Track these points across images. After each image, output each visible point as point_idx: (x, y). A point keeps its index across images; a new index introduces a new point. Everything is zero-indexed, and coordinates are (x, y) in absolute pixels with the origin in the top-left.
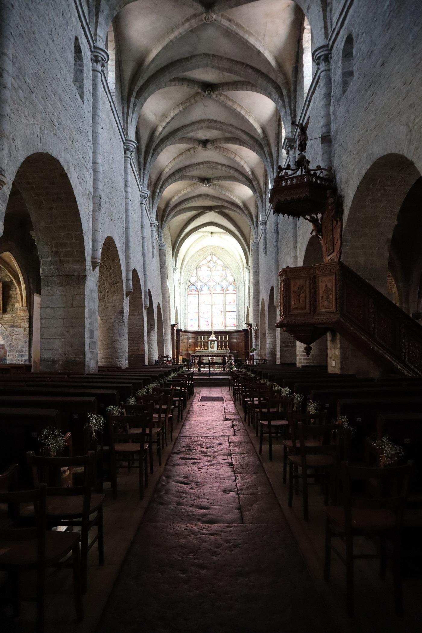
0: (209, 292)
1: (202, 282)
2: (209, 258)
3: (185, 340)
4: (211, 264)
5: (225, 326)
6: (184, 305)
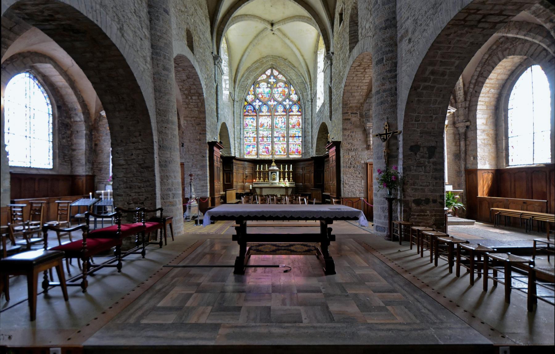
0: (269, 114)
1: (260, 101)
2: (269, 72)
3: (241, 171)
4: (272, 80)
6: (239, 128)
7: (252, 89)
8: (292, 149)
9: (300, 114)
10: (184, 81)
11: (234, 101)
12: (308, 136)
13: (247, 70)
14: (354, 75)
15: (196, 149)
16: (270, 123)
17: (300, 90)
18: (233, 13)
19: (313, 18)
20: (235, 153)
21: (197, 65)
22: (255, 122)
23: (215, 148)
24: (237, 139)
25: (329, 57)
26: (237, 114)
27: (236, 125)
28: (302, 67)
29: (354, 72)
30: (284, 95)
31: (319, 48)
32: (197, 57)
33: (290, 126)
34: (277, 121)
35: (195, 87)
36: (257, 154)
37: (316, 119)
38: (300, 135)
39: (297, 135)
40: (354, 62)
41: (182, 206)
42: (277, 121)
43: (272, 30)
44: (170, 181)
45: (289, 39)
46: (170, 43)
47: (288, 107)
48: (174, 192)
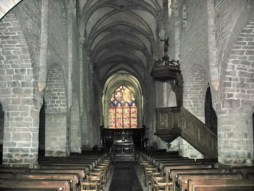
0: (121, 107)
1: (117, 101)
2: (121, 87)
5: (130, 126)
6: (107, 114)
9: (136, 107)
12: (140, 118)
16: (122, 111)
36: (116, 126)
38: (136, 117)
47: (130, 103)
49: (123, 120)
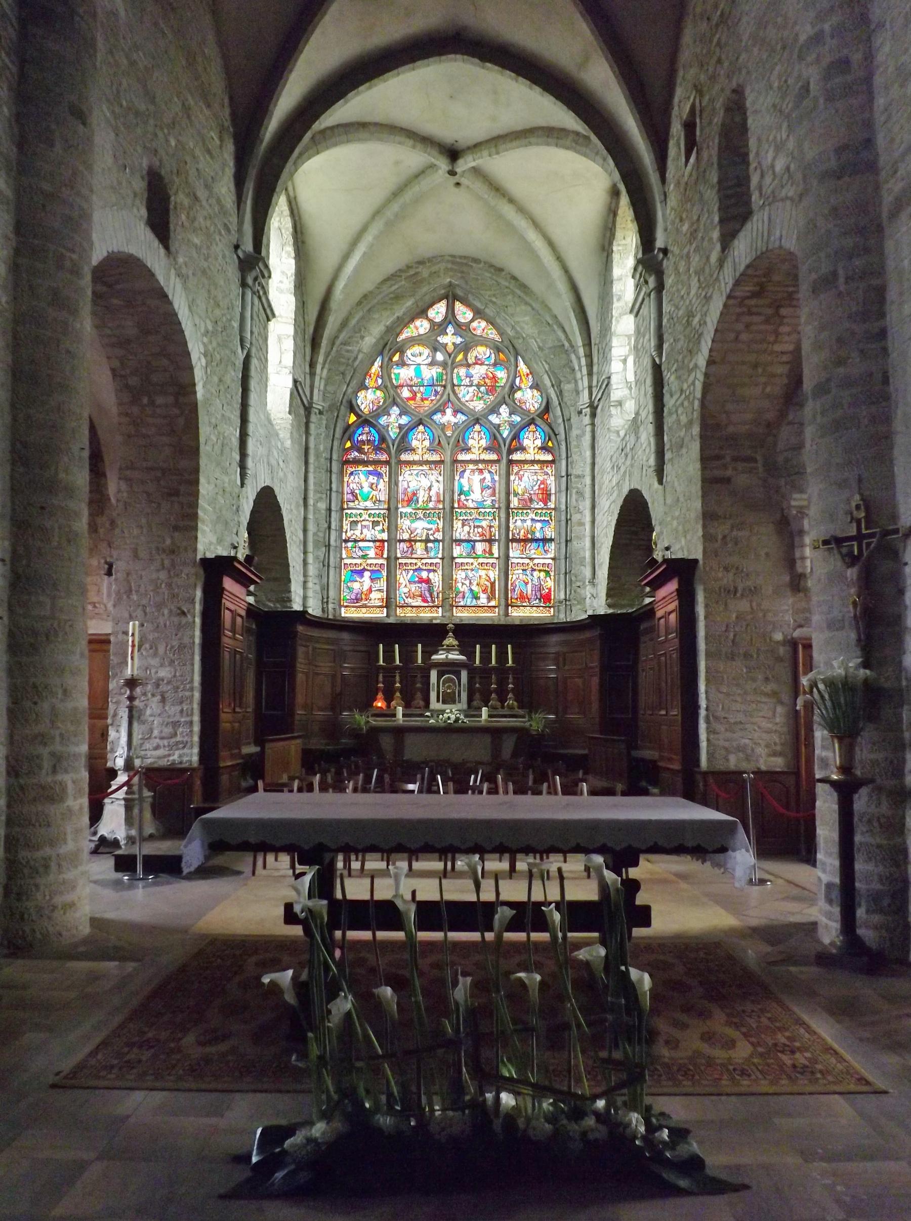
0: (436, 457)
2: (438, 312)
3: (325, 666)
4: (450, 339)
6: (322, 506)
7: (376, 368)
8: (519, 585)
10: (128, 341)
11: (308, 410)
12: (580, 538)
13: (359, 303)
14: (740, 326)
15: (157, 587)
16: (438, 488)
17: (552, 373)
18: (317, 117)
19: (594, 138)
20: (305, 598)
21: (179, 286)
22: (382, 485)
23: (228, 584)
24: (316, 544)
25: (650, 262)
26: (317, 456)
27: (311, 494)
28: (559, 295)
29: (739, 315)
30: (491, 390)
31: (619, 234)
32: (181, 260)
33: (515, 502)
34: (464, 481)
35: (165, 362)
36: (389, 603)
37: (606, 478)
39: (538, 535)
40: (737, 283)
41: (85, 801)
42: (464, 481)
43: (452, 173)
44: (45, 706)
45: (511, 201)
46: (86, 216)
48: (58, 747)
49: (449, 561)
